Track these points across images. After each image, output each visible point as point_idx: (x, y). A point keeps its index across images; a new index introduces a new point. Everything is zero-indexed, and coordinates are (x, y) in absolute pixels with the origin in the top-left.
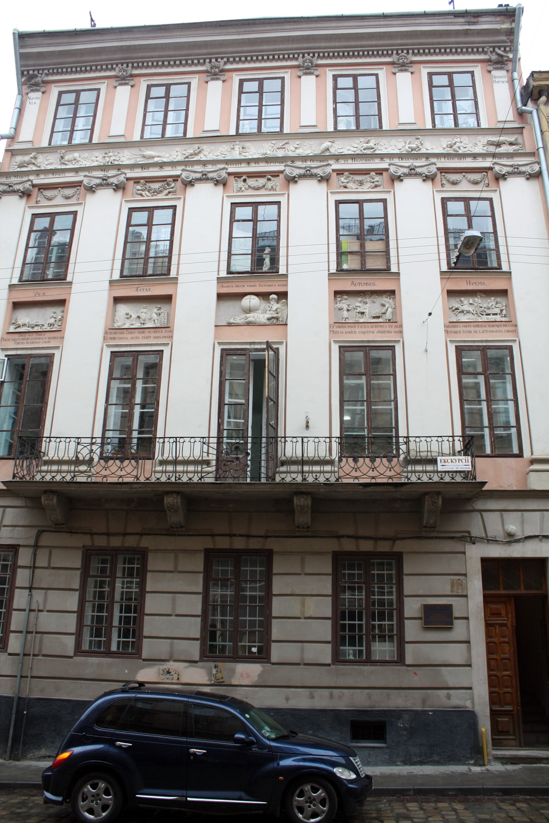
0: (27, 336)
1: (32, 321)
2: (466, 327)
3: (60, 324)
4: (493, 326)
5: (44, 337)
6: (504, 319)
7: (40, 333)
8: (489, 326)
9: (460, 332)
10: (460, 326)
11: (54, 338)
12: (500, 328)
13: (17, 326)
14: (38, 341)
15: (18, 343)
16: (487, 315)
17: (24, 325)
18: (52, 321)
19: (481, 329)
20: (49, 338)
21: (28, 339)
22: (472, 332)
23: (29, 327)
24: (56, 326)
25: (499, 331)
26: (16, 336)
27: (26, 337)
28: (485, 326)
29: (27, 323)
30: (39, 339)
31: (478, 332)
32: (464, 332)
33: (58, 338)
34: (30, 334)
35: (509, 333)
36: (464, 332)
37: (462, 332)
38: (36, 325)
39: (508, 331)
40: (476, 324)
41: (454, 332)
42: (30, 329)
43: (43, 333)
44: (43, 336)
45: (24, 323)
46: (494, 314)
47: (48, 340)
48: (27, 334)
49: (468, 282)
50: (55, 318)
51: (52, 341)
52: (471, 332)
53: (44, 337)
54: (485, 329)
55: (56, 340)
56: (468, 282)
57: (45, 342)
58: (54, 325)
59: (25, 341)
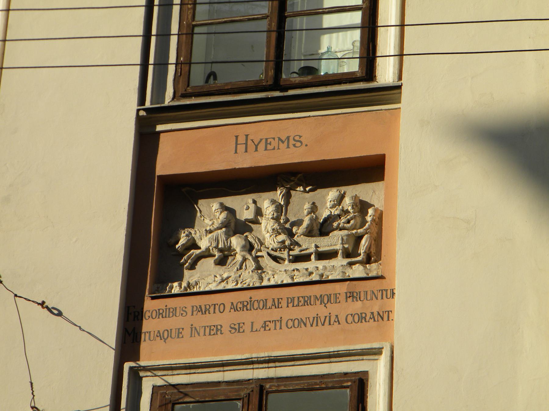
2: (203, 310)
4: (307, 301)
6: (358, 271)
8: (291, 301)
9: (179, 333)
10: (184, 309)
12: (333, 309)
16: (297, 259)
19: (259, 316)
22: (226, 329)
25: (328, 320)
28: (277, 304)
31: (247, 327)
32: (194, 330)
35: (364, 325)
36: (194, 330)
37: (186, 332)
39: (362, 318)
40: (245, 296)
41: (160, 335)
46: (322, 256)
49: (242, 140)
52: (217, 330)
54: (275, 314)
56: (242, 140)
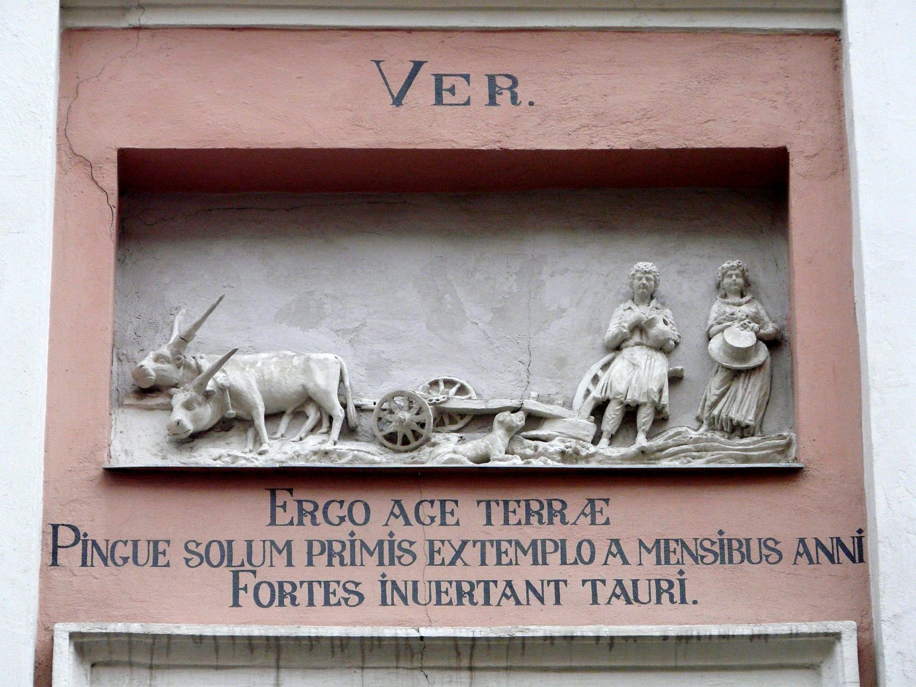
0: (378, 517)
1: (377, 368)
3: (742, 405)
5: (600, 536)
7: (538, 495)
11: (726, 550)
13: (207, 414)
14: (525, 572)
15: (282, 595)
17: (294, 408)
18: (638, 374)
20: (662, 550)
21: (390, 551)
23: (349, 431)
24: (685, 427)
26: (241, 518)
27: (372, 533)
29: (324, 382)
30: (538, 553)
33: (770, 550)
34: (410, 499)
38: (446, 417)
42: (368, 454)
43: (575, 500)
44: (574, 518)
45: (290, 382)
47: (647, 569)
48: (381, 503)
50: (664, 348)
51: (702, 579)
53: (600, 536)
55: (755, 573)
57: (627, 594)
58: (660, 419)
59: (368, 575)
